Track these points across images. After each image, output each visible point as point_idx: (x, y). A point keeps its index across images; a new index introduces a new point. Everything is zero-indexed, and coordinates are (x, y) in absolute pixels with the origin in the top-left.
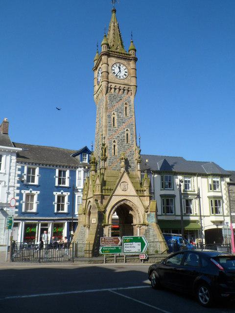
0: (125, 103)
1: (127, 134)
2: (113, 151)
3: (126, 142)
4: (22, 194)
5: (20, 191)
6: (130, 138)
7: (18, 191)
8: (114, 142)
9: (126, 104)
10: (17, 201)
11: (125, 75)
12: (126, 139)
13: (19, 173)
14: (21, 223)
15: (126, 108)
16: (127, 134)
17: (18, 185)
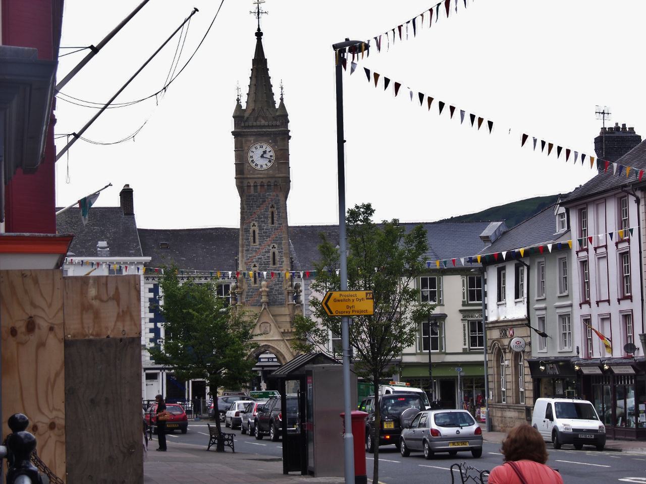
0: (270, 205)
1: (274, 253)
2: (253, 279)
3: (271, 266)
4: (159, 329)
5: (155, 325)
6: (277, 258)
7: (152, 325)
8: (255, 266)
9: (272, 207)
10: (151, 340)
12: (271, 260)
13: (151, 295)
14: (161, 373)
15: (272, 213)
16: (274, 253)
17: (152, 315)
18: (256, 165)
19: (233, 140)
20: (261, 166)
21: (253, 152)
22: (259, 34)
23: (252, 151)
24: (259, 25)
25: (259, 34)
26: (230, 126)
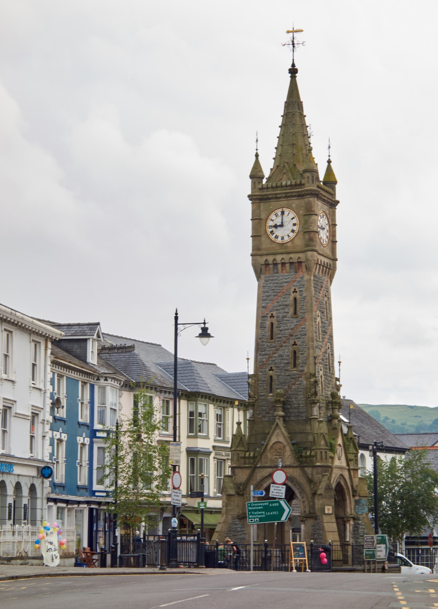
11: (293, 231)
18: (277, 237)
19: (251, 205)
20: (283, 238)
21: (273, 220)
22: (293, 71)
23: (271, 220)
24: (293, 60)
25: (293, 71)
26: (247, 187)
